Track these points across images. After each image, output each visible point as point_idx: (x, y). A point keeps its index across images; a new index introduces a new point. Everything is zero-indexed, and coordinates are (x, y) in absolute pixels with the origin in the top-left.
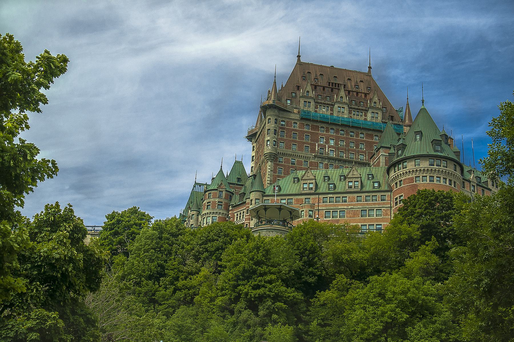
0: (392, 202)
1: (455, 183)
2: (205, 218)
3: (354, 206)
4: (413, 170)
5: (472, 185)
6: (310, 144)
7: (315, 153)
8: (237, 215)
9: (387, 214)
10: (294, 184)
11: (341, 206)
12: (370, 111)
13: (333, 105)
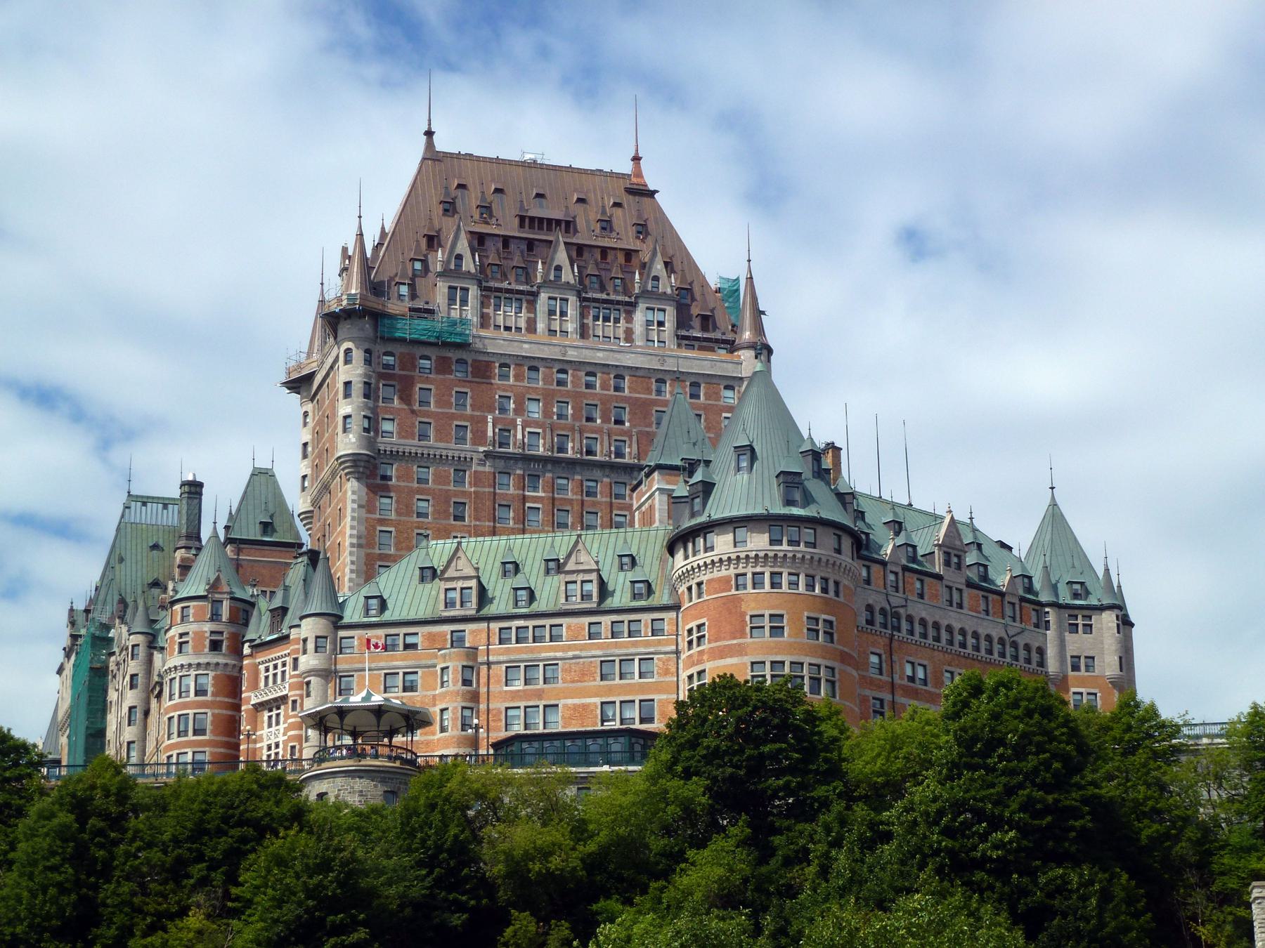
0: (680, 639)
1: (837, 583)
2: (175, 678)
3: (581, 650)
4: (729, 558)
5: (891, 572)
6: (471, 418)
7: (483, 444)
8: (267, 670)
9: (667, 672)
10: (421, 586)
11: (546, 651)
12: (642, 305)
13: (535, 295)
